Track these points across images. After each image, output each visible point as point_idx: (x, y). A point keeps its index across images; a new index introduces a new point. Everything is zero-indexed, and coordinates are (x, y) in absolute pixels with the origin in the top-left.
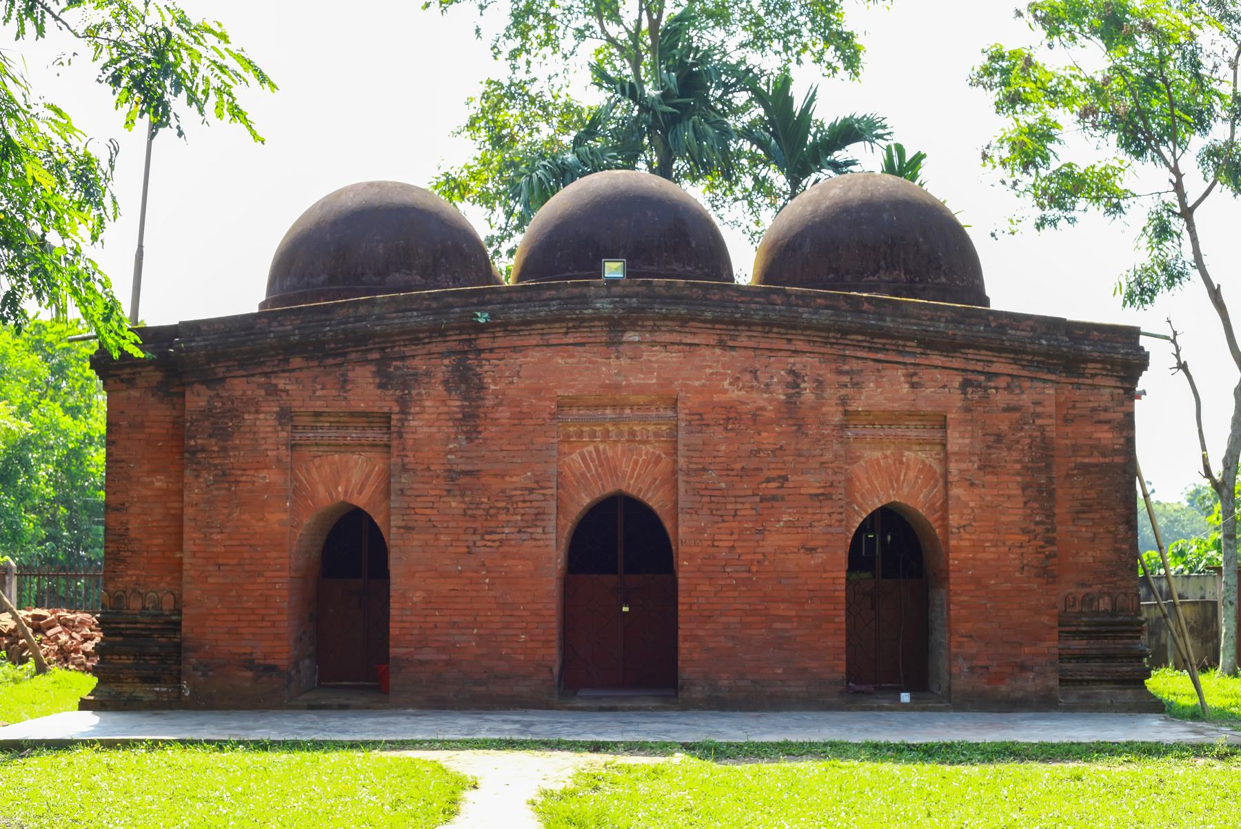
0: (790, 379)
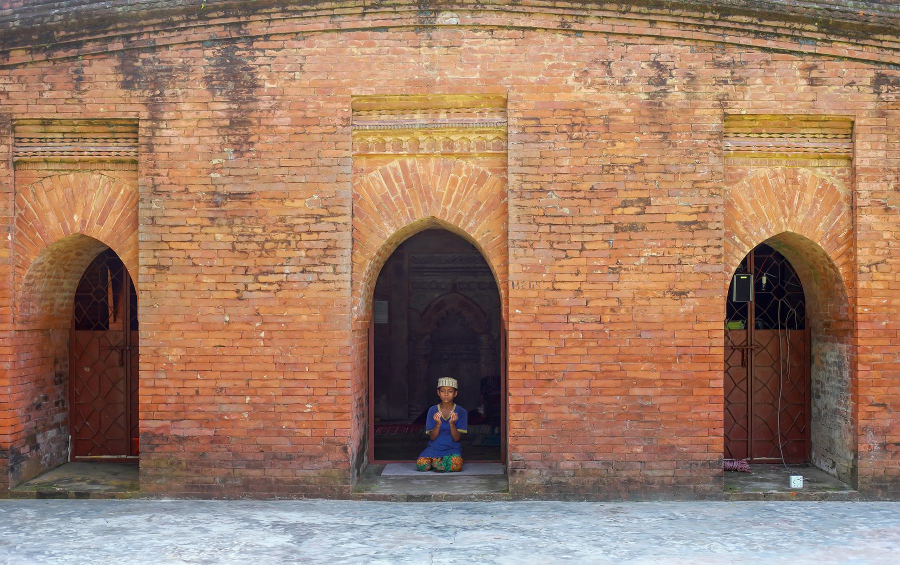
0: (653, 73)
